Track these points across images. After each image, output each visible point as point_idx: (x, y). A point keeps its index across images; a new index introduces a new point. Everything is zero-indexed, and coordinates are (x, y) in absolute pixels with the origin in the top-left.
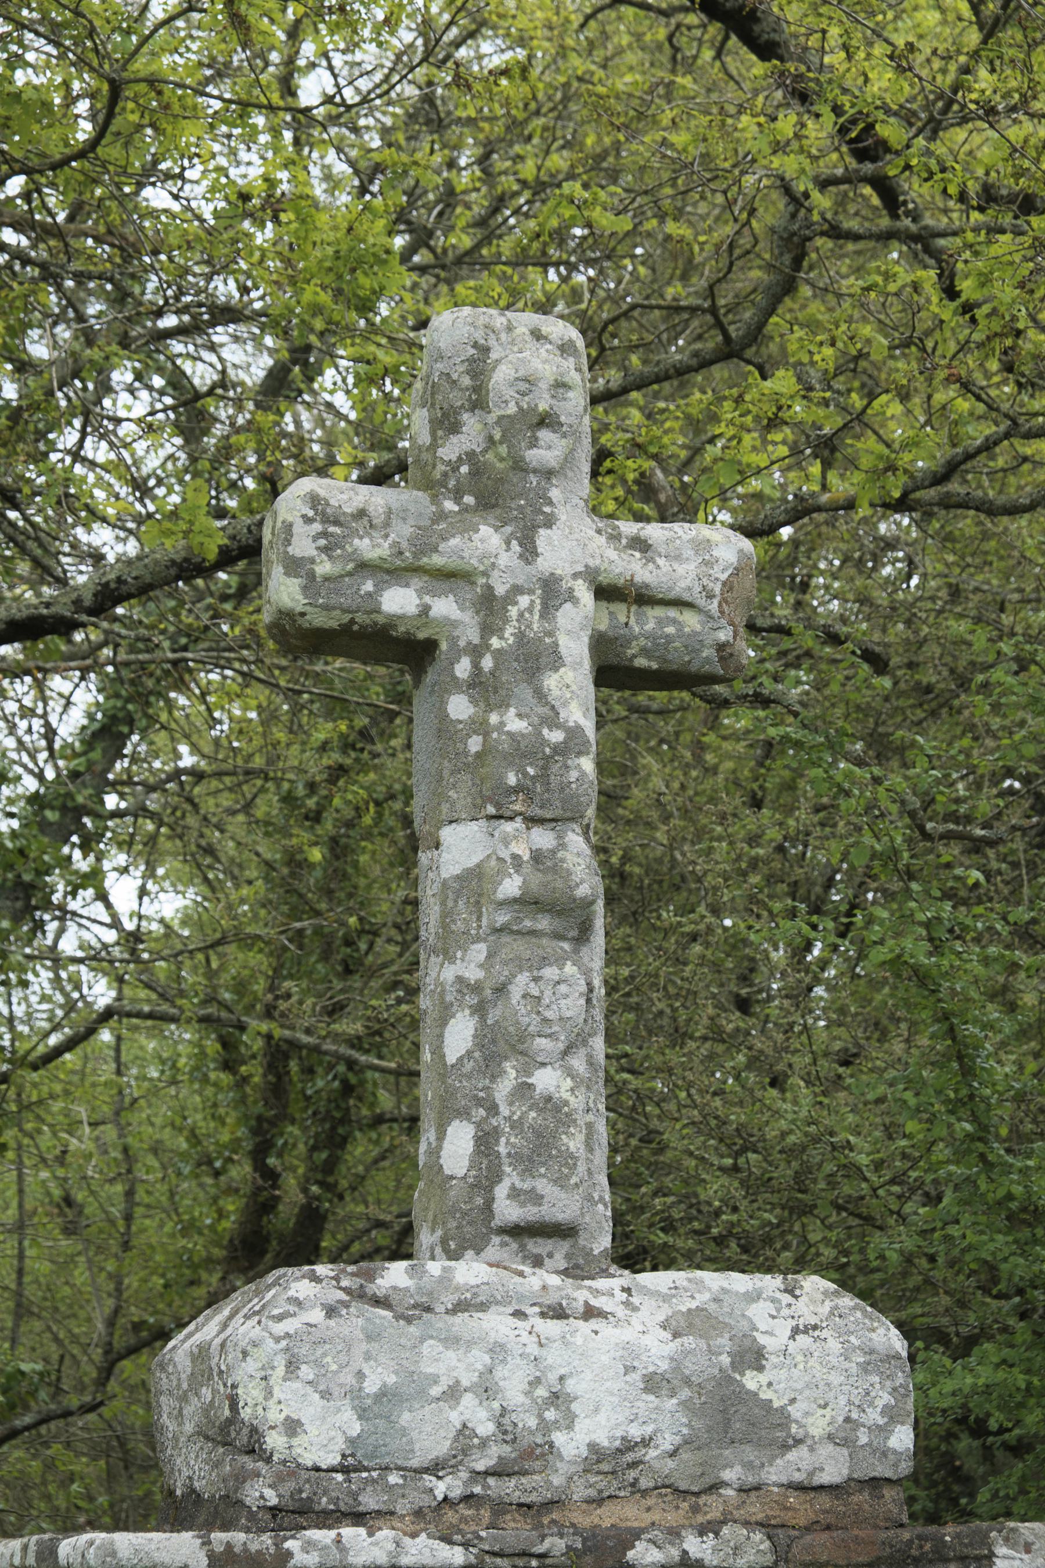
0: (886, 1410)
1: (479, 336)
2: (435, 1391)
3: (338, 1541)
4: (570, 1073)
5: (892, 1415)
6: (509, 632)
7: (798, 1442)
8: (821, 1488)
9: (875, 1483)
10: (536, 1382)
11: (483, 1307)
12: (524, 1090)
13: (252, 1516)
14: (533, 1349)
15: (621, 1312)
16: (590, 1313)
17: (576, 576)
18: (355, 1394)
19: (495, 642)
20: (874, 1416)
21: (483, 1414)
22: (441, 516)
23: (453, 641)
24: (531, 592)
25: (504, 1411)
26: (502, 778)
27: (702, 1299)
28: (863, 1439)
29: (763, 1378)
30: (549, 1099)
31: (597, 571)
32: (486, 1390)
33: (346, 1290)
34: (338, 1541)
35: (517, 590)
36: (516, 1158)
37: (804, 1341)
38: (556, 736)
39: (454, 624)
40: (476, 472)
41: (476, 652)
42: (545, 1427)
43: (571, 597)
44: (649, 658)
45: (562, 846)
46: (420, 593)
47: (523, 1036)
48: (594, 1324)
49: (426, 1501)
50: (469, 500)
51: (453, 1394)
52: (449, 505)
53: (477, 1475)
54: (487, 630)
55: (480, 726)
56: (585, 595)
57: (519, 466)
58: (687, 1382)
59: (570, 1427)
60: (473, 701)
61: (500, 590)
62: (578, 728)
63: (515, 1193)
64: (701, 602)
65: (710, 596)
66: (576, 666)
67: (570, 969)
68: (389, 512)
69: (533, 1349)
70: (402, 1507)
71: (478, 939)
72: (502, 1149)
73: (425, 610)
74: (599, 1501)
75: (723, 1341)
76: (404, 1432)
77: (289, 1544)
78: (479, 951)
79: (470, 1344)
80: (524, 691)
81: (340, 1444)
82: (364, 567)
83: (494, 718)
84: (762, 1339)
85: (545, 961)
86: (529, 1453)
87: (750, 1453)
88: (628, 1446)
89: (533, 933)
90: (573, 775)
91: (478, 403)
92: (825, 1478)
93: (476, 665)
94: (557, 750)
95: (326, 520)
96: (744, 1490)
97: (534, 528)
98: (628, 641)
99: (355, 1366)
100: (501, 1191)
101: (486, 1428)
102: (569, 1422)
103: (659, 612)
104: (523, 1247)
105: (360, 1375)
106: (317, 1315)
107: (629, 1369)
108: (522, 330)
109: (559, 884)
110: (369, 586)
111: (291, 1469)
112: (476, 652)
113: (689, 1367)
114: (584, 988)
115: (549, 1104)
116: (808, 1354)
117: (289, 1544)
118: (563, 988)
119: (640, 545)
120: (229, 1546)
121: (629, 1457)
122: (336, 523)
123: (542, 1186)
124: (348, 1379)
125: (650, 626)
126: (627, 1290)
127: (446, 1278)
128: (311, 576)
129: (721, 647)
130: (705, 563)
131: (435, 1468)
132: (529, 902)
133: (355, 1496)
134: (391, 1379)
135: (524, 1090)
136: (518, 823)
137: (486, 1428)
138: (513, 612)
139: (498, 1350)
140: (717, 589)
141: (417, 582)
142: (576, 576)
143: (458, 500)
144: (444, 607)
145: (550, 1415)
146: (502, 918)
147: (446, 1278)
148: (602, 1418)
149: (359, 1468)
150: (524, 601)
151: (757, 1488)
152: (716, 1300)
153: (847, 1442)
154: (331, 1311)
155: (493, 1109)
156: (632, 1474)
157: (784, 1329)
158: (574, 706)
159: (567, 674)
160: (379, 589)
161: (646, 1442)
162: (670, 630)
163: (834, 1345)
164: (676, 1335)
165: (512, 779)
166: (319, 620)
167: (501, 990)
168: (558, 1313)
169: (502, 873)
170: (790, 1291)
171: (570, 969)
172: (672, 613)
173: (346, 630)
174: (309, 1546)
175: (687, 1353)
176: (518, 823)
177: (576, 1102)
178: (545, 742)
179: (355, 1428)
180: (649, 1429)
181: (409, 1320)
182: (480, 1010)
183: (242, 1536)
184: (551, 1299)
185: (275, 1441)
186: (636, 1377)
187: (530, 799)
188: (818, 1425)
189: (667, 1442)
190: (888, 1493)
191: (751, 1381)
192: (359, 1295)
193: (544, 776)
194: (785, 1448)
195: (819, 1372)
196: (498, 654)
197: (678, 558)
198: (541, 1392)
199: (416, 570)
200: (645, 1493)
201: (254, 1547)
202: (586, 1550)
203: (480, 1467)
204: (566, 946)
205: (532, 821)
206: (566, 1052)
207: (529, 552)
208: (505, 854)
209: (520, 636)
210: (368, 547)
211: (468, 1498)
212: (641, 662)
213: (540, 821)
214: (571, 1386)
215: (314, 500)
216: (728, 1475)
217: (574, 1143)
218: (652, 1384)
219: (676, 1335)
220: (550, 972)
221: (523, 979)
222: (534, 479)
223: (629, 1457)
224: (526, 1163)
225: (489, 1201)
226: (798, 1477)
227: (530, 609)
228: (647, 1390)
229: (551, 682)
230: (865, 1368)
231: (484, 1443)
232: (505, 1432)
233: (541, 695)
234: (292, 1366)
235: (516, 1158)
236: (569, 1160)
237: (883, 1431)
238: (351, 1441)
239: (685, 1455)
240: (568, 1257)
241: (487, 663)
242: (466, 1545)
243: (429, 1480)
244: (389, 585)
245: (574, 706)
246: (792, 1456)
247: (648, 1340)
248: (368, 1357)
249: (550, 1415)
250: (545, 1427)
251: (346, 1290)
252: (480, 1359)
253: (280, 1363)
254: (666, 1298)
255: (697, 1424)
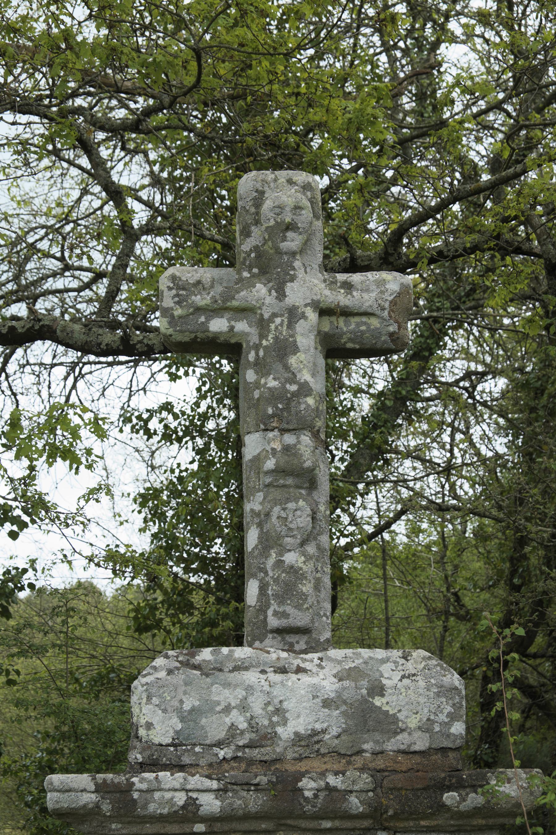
0: (449, 715)
1: (259, 186)
2: (218, 708)
3: (157, 778)
4: (304, 554)
5: (453, 717)
6: (271, 336)
7: (402, 730)
8: (415, 752)
9: (444, 750)
10: (268, 704)
11: (247, 669)
12: (279, 563)
13: (132, 767)
14: (267, 688)
15: (315, 669)
16: (299, 670)
17: (306, 305)
18: (179, 711)
19: (264, 343)
20: (443, 718)
21: (242, 719)
22: (241, 280)
23: (248, 342)
24: (282, 315)
25: (252, 717)
26: (265, 410)
27: (358, 662)
28: (437, 728)
29: (384, 700)
30: (292, 567)
31: (319, 302)
32: (243, 707)
33: (180, 662)
34: (157, 778)
35: (274, 315)
36: (276, 596)
37: (406, 681)
38: (294, 388)
39: (247, 334)
40: (258, 257)
41: (257, 347)
42: (272, 725)
43: (303, 316)
44: (354, 343)
45: (299, 442)
46: (229, 320)
47: (279, 537)
48: (300, 676)
49: (214, 759)
50: (255, 270)
51: (227, 709)
52: (246, 274)
53: (239, 748)
54: (262, 336)
55: (257, 385)
56: (312, 316)
57: (279, 252)
58: (345, 702)
59: (285, 724)
60: (257, 373)
61: (266, 316)
62: (306, 382)
63: (276, 613)
64: (378, 312)
65: (383, 309)
66: (306, 351)
67: (301, 503)
68: (213, 281)
69: (267, 688)
70: (203, 762)
71: (259, 491)
72: (270, 592)
73: (232, 328)
74: (300, 759)
75: (364, 683)
76: (203, 728)
77: (135, 780)
78: (260, 496)
79: (236, 686)
80: (279, 367)
81: (171, 733)
82: (198, 310)
83: (263, 381)
84: (384, 681)
85: (288, 500)
86: (265, 737)
87: (377, 736)
88: (315, 733)
89: (284, 486)
90: (303, 407)
91: (257, 222)
92: (417, 748)
93: (257, 354)
94: (295, 394)
95: (179, 288)
96: (375, 754)
97: (284, 283)
98: (341, 336)
99: (178, 698)
100: (270, 612)
101: (243, 725)
102: (285, 722)
103: (357, 319)
104: (283, 639)
105: (181, 702)
106: (162, 674)
107: (314, 697)
108: (282, 180)
109: (296, 461)
110: (202, 319)
111: (149, 745)
112: (257, 347)
113: (345, 695)
114: (308, 511)
115: (293, 570)
116: (407, 688)
117: (135, 780)
118: (298, 513)
119: (348, 286)
120: (105, 780)
121: (316, 738)
122: (184, 289)
123: (289, 609)
124: (176, 704)
125: (353, 326)
126: (321, 659)
127: (230, 655)
128: (172, 316)
129: (391, 335)
130: (382, 292)
131: (219, 744)
132: (278, 471)
133: (179, 757)
134: (197, 703)
135: (279, 563)
136: (276, 432)
137: (243, 725)
138: (273, 326)
139: (249, 689)
140: (387, 305)
141: (227, 315)
142: (306, 305)
143: (250, 271)
144: (241, 326)
145: (275, 719)
146: (268, 480)
147: (230, 655)
148: (301, 720)
149: (181, 745)
150: (278, 320)
151: (382, 752)
152: (366, 663)
153: (427, 731)
154: (170, 672)
155: (266, 573)
156: (317, 747)
157: (397, 676)
158: (305, 372)
159: (301, 356)
160: (208, 320)
161: (324, 731)
162: (363, 328)
163: (422, 684)
164: (340, 680)
165: (270, 411)
166: (179, 338)
167: (268, 515)
168: (283, 671)
169: (267, 458)
170: (405, 658)
171: (301, 503)
172: (364, 319)
173: (194, 341)
174: (142, 780)
175: (344, 689)
176: (276, 432)
177: (308, 568)
178: (287, 391)
179: (179, 726)
180: (325, 725)
181: (207, 675)
182: (260, 525)
183: (110, 776)
184: (280, 664)
185: (142, 732)
186: (318, 700)
187: (281, 420)
188: (413, 722)
189: (334, 731)
190: (451, 755)
191: (378, 701)
192: (187, 664)
193: (287, 408)
194: (396, 733)
195: (413, 697)
196: (266, 348)
197: (368, 290)
198: (271, 708)
199: (226, 309)
200: (323, 755)
201: (116, 781)
202: (278, 782)
203: (241, 743)
204: (303, 492)
205: (283, 431)
206: (303, 544)
207: (281, 295)
208: (268, 448)
209: (276, 338)
210: (200, 300)
211: (235, 758)
212: (350, 345)
213: (288, 431)
214: (285, 705)
215: (173, 278)
216: (366, 746)
217: (307, 588)
218: (327, 703)
219: (340, 680)
220: (291, 505)
221: (277, 510)
222: (286, 258)
223: (316, 738)
224: (281, 599)
225: (266, 617)
226: (402, 747)
227: (281, 324)
228: (324, 707)
229: (293, 361)
230: (438, 694)
231: (242, 732)
232: (253, 726)
233: (287, 368)
234: (149, 698)
235: (276, 596)
236: (304, 597)
237: (448, 725)
238: (177, 732)
239: (343, 737)
240: (307, 643)
241: (261, 353)
242: (218, 780)
243: (216, 750)
244: (212, 317)
245: (305, 372)
246: (399, 737)
247: (324, 683)
248: (185, 693)
249: (275, 719)
250: (272, 725)
251: (180, 662)
252: (241, 693)
253: (144, 696)
254: (339, 662)
255: (350, 723)
